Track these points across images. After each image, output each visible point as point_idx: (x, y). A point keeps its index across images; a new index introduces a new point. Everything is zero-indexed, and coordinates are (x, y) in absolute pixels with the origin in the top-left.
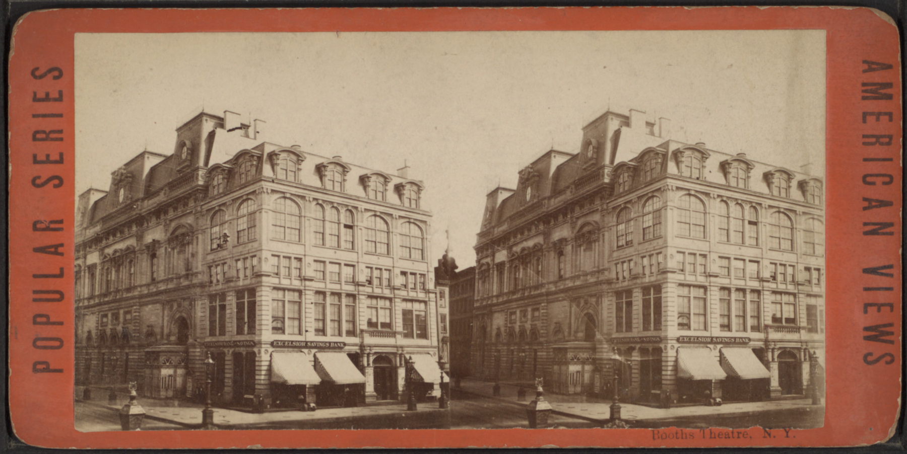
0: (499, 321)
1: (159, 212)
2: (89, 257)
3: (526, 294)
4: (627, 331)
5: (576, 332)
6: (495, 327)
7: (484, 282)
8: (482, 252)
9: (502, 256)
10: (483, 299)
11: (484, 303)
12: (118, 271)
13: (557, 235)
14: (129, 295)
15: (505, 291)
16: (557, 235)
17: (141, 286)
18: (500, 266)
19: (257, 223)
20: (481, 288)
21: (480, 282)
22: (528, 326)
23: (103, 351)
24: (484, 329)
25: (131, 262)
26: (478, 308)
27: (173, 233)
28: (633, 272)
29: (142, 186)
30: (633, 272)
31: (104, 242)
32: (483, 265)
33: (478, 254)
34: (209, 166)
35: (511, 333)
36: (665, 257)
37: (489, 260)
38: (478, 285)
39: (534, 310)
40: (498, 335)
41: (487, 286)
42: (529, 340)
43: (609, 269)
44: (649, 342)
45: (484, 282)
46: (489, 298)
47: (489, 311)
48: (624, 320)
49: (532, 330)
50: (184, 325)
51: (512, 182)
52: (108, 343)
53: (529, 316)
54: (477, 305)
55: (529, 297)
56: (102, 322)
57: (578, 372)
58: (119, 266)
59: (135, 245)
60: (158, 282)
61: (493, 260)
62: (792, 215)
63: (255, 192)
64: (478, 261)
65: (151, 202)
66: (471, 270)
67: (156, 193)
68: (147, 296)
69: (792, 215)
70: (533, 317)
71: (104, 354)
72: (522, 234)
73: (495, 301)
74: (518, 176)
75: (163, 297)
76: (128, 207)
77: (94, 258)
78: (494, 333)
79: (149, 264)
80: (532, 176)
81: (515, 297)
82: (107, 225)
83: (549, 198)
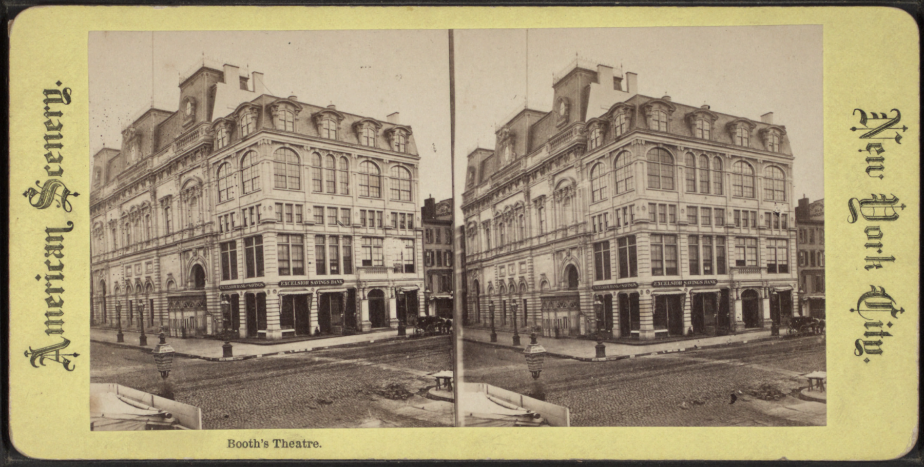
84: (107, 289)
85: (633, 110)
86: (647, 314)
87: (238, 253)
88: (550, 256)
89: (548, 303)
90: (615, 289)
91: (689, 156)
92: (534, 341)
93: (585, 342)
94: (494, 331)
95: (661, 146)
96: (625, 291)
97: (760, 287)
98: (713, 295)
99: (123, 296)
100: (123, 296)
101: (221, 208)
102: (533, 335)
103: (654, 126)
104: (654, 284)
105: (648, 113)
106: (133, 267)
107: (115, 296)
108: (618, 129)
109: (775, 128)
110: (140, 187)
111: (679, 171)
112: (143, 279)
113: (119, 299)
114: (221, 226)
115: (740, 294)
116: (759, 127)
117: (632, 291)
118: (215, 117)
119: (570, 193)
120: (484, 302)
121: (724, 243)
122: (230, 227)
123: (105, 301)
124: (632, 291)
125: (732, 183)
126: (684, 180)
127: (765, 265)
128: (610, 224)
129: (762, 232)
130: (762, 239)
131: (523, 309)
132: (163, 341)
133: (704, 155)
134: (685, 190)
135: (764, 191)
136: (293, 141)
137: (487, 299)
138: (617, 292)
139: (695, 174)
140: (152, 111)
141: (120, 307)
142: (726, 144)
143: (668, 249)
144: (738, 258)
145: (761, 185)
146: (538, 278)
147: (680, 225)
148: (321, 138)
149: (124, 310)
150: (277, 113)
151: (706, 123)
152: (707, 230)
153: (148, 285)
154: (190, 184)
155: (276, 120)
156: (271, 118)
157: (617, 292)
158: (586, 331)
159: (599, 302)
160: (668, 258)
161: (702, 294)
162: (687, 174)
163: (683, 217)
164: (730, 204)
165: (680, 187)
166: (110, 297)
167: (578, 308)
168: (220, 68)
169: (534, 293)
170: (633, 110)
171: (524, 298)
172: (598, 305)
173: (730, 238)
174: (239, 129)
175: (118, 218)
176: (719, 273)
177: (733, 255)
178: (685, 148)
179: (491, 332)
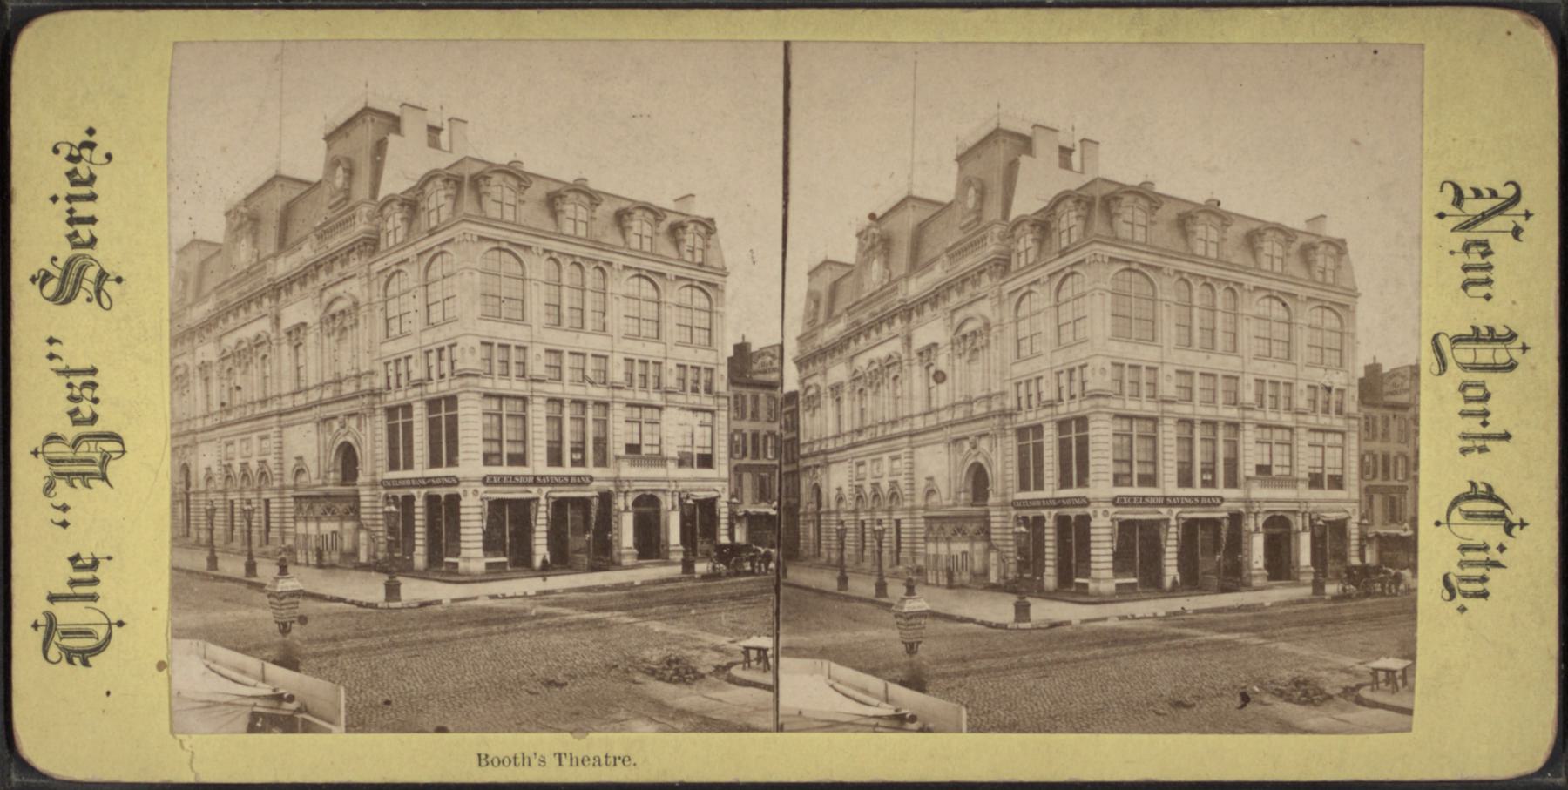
9: (839, 372)
10: (812, 443)
18: (836, 389)
33: (800, 370)
38: (805, 420)
45: (813, 415)
64: (802, 382)
73: (831, 446)
85: (1090, 204)
88: (941, 447)
90: (1051, 507)
92: (910, 591)
93: (997, 595)
102: (910, 580)
108: (1065, 235)
117: (1080, 511)
118: (1015, 213)
119: (979, 342)
122: (1034, 401)
123: (819, 521)
124: (1080, 511)
128: (1046, 396)
136: (1145, 258)
137: (833, 518)
139: (1191, 317)
147: (1164, 401)
148: (1194, 255)
156: (1110, 216)
159: (1023, 529)
160: (1143, 457)
163: (1168, 388)
168: (1026, 130)
169: (912, 509)
171: (896, 516)
174: (1055, 235)
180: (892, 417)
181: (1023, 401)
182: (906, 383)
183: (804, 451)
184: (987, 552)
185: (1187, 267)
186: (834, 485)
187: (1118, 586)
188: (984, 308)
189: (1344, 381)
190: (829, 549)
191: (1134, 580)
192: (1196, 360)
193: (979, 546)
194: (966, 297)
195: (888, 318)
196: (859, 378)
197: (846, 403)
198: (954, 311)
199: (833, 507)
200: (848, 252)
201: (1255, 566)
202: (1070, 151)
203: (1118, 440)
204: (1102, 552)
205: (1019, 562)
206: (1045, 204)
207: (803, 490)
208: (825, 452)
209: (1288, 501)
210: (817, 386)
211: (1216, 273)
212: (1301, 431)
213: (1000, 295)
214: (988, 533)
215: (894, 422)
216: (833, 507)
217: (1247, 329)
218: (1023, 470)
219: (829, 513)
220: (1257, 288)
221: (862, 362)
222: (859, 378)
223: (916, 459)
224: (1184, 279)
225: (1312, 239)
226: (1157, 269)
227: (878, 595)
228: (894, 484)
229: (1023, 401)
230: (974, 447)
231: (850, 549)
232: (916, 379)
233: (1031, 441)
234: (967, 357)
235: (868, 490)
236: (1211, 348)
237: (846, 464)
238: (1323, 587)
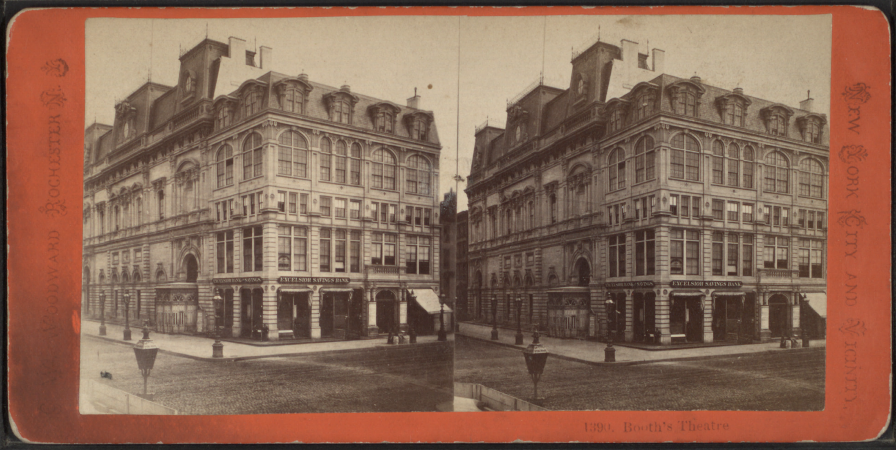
0: (493, 267)
1: (557, 150)
2: (97, 195)
3: (519, 240)
4: (620, 276)
5: (570, 277)
6: (490, 272)
7: (477, 227)
8: (473, 196)
9: (493, 200)
10: (477, 244)
11: (479, 248)
12: (518, 213)
13: (549, 177)
14: (530, 237)
15: (499, 235)
16: (549, 177)
17: (149, 224)
18: (492, 210)
19: (264, 161)
20: (474, 233)
21: (474, 227)
22: (523, 271)
23: (116, 289)
24: (479, 275)
25: (531, 203)
26: (474, 253)
27: (179, 169)
28: (627, 217)
29: (537, 124)
30: (627, 217)
31: (503, 182)
32: (475, 208)
33: (469, 197)
34: (607, 101)
35: (506, 279)
36: (659, 200)
37: (480, 204)
38: (472, 230)
39: (529, 255)
40: (494, 281)
41: (480, 231)
42: (513, 285)
43: (600, 214)
44: (643, 287)
45: (477, 227)
46: (482, 243)
47: (483, 256)
48: (617, 266)
49: (527, 274)
50: (583, 269)
51: (500, 121)
52: (121, 281)
53: (524, 262)
54: (471, 250)
55: (522, 242)
56: (506, 265)
57: (573, 316)
58: (127, 204)
59: (534, 186)
60: (166, 220)
61: (485, 203)
62: (789, 156)
63: (653, 128)
64: (470, 205)
65: (548, 141)
66: (464, 214)
67: (553, 131)
68: (548, 238)
69: (789, 156)
70: (528, 262)
71: (509, 296)
72: (513, 176)
73: (489, 246)
74: (506, 114)
75: (172, 235)
76: (526, 147)
77: (102, 196)
78: (490, 278)
79: (549, 207)
80: (518, 113)
81: (509, 242)
82: (115, 161)
83: (539, 139)
84: (92, 276)
85: (266, 89)
86: (270, 313)
87: (235, 244)
88: (168, 244)
89: (163, 295)
90: (238, 283)
91: (325, 142)
92: (146, 336)
93: (202, 339)
94: (127, 326)
95: (294, 129)
96: (248, 286)
97: (790, 293)
98: (347, 293)
99: (108, 285)
100: (108, 285)
101: (217, 195)
102: (145, 329)
103: (288, 108)
104: (671, 284)
105: (281, 93)
106: (120, 253)
107: (100, 285)
108: (249, 109)
109: (815, 117)
110: (133, 168)
111: (313, 157)
112: (131, 269)
113: (104, 288)
114: (218, 214)
115: (767, 299)
116: (797, 115)
117: (257, 286)
118: (217, 94)
119: (193, 177)
120: (94, 291)
121: (306, 234)
122: (228, 216)
123: (88, 290)
124: (257, 286)
125: (371, 172)
126: (319, 167)
127: (796, 268)
128: (236, 212)
129: (795, 231)
130: (795, 239)
131: (136, 300)
132: (146, 336)
133: (342, 141)
134: (711, 182)
135: (798, 186)
136: (301, 123)
138: (239, 287)
139: (330, 162)
140: (148, 86)
141: (105, 297)
142: (367, 130)
143: (297, 243)
144: (374, 256)
145: (795, 180)
146: (154, 268)
147: (311, 216)
148: (332, 122)
149: (108, 300)
150: (285, 93)
151: (344, 106)
152: (733, 226)
153: (137, 275)
154: (187, 167)
155: (285, 100)
157: (239, 287)
158: (203, 328)
159: (219, 297)
160: (297, 252)
161: (725, 296)
162: (322, 160)
163: (315, 208)
164: (367, 195)
165: (314, 173)
166: (94, 285)
167: (196, 303)
169: (149, 284)
170: (266, 89)
171: (138, 288)
172: (217, 300)
173: (366, 233)
174: (242, 110)
175: (107, 199)
176: (352, 271)
177: (762, 254)
178: (322, 133)
179: (123, 328)
180: (529, 228)
181: (614, 221)
182: (537, 207)
183: (471, 250)
184: (588, 316)
185: (721, 133)
186: (490, 272)
187: (673, 339)
188: (588, 158)
189: (825, 208)
190: (486, 313)
191: (684, 335)
192: (724, 192)
193: (583, 312)
194: (577, 152)
195: (526, 164)
196: (507, 203)
197: (498, 221)
198: (569, 160)
199: (489, 286)
200: (500, 121)
201: (762, 327)
202: (646, 57)
203: (674, 245)
204: (663, 317)
205: (217, 319)
206: (628, 91)
207: (470, 275)
208: (485, 250)
209: (783, 285)
210: (480, 208)
211: (738, 136)
212: (795, 239)
213: (598, 150)
214: (589, 304)
215: (529, 232)
216: (97, 282)
217: (759, 175)
218: (612, 263)
219: (487, 289)
220: (766, 146)
221: (509, 193)
222: (507, 203)
223: (544, 256)
224: (719, 141)
225: (804, 114)
226: (701, 134)
227: (517, 343)
228: (528, 272)
229: (614, 221)
230: (580, 248)
231: (499, 314)
232: (544, 204)
233: (617, 245)
234: (577, 190)
235: (512, 274)
236: (736, 186)
237: (498, 258)
238: (808, 342)
